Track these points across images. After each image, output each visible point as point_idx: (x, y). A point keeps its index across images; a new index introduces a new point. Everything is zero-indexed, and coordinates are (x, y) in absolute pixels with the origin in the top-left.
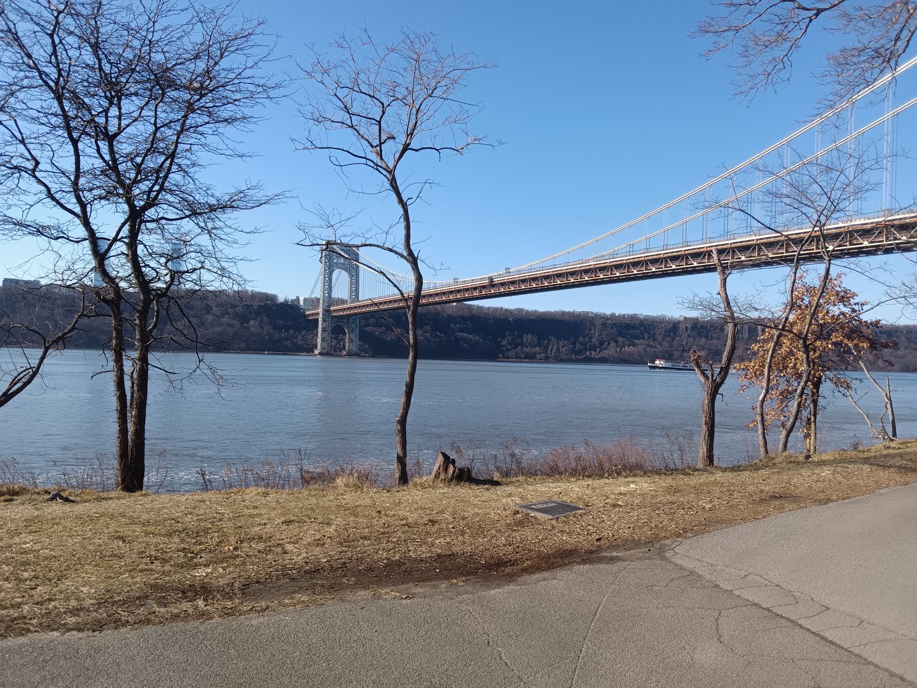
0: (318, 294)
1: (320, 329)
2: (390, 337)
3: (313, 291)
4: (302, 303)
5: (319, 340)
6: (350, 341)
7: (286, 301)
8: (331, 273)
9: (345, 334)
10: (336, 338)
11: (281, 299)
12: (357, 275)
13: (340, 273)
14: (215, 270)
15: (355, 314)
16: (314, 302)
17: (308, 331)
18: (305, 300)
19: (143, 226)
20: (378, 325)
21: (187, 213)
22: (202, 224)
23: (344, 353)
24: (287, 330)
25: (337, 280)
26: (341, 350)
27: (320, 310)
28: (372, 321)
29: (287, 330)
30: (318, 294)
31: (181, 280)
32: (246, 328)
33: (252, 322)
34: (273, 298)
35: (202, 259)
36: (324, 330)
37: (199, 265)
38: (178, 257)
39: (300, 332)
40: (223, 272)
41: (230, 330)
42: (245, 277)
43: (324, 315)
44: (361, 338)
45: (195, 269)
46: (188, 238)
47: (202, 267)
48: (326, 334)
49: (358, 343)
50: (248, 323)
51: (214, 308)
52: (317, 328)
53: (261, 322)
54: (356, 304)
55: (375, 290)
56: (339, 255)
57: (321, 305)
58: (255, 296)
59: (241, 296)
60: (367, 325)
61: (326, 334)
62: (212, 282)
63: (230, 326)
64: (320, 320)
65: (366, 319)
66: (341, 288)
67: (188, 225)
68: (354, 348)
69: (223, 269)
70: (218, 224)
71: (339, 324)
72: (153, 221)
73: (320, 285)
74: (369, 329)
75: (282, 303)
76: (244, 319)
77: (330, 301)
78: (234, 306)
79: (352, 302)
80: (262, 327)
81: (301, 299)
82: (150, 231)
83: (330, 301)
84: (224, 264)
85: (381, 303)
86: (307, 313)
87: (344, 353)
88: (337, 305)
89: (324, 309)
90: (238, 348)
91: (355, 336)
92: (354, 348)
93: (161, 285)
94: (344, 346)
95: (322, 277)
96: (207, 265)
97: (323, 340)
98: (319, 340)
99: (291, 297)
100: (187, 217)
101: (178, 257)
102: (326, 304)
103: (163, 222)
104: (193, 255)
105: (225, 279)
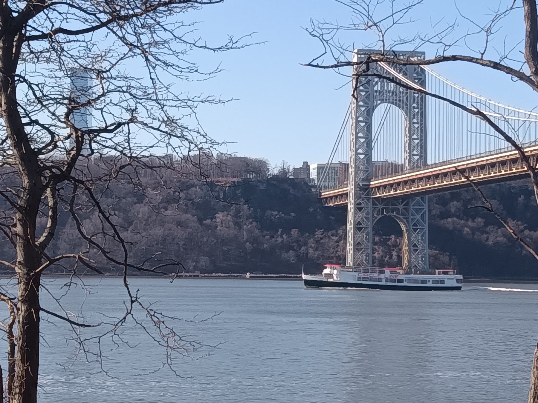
0: (345, 155)
1: (350, 227)
2: (494, 237)
3: (335, 151)
4: (313, 174)
5: (349, 248)
7: (284, 172)
8: (369, 112)
9: (400, 234)
10: (383, 243)
11: (274, 169)
13: (387, 110)
14: (156, 124)
15: (422, 194)
16: (335, 172)
17: (327, 230)
18: (320, 168)
19: (24, 49)
20: (468, 213)
21: (104, 17)
22: (132, 39)
24: (287, 231)
25: (381, 125)
27: (350, 188)
28: (454, 206)
29: (287, 231)
30: (345, 155)
31: (94, 145)
32: (208, 227)
33: (220, 216)
34: (258, 167)
35: (132, 104)
36: (358, 228)
37: (127, 116)
38: (89, 103)
39: (313, 233)
40: (171, 127)
41: (180, 233)
42: (211, 135)
44: (432, 243)
45: (119, 125)
46: (106, 65)
47: (132, 120)
48: (362, 236)
49: (427, 251)
50: (213, 218)
51: (150, 191)
52: (344, 222)
53: (237, 215)
55: (458, 144)
56: (386, 77)
57: (352, 177)
58: (226, 164)
59: (203, 168)
60: (445, 215)
61: (362, 236)
62: (146, 142)
63: (179, 224)
64: (351, 207)
65: (443, 202)
66: (391, 142)
67: (104, 40)
69: (170, 121)
70: (160, 35)
71: (387, 216)
72: (43, 36)
73: (349, 137)
74: (449, 222)
75: (275, 177)
76: (205, 211)
78: (185, 187)
79: (413, 169)
80: (239, 225)
81: (313, 167)
82: (37, 55)
83: (369, 168)
84: (173, 113)
85: (473, 169)
86: (325, 194)
88: (383, 176)
89: (357, 186)
90: (196, 268)
91: (421, 239)
93: (58, 155)
94: (400, 258)
95: (352, 122)
96: (142, 115)
97: (357, 247)
98: (349, 248)
99: (294, 163)
100: (103, 25)
101: (89, 103)
102: (362, 175)
103: (61, 37)
104: (115, 97)
105: (175, 141)
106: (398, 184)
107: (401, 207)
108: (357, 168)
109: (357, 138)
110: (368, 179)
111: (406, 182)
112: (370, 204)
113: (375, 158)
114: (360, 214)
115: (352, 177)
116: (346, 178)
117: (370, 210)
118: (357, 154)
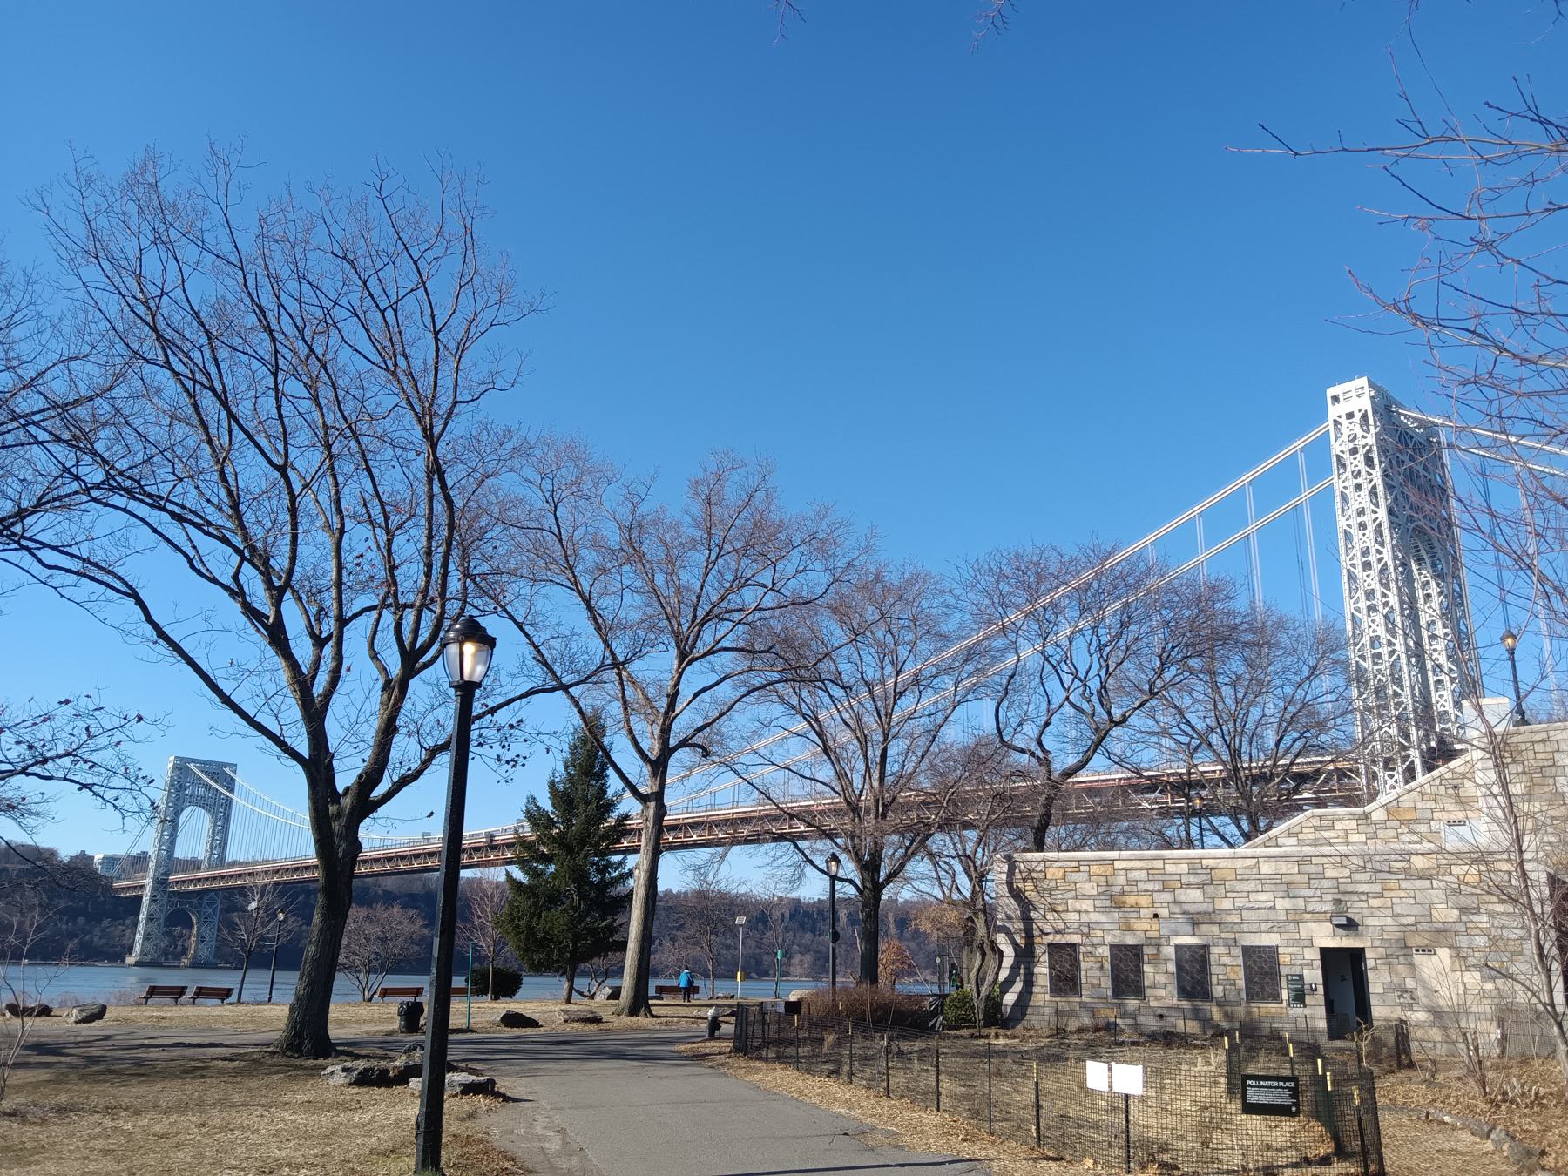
9: (190, 926)
12: (227, 817)
16: (139, 861)
17: (115, 918)
26: (178, 956)
27: (148, 881)
43: (154, 889)
54: (216, 873)
68: (206, 953)
77: (169, 863)
83: (169, 863)
91: (209, 933)
92: (206, 953)
110: (167, 874)
116: (146, 869)
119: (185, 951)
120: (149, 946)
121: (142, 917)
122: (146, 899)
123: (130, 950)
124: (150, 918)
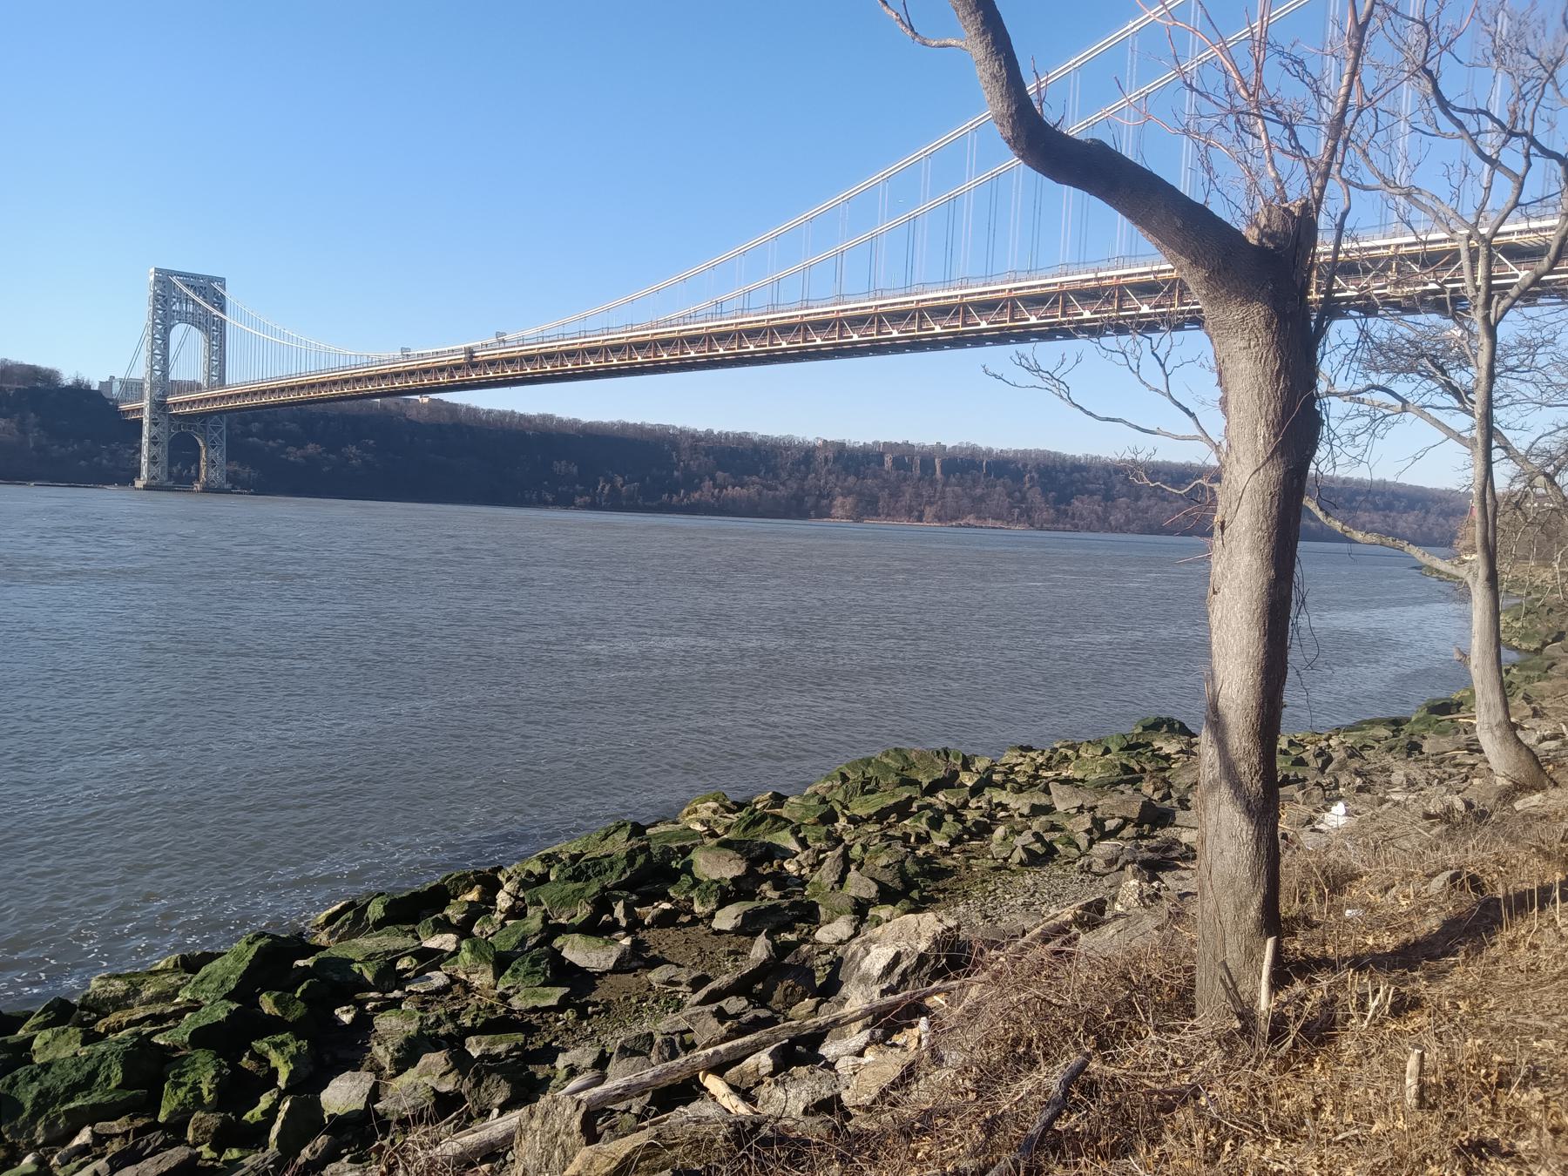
0: (140, 372)
3: (131, 366)
6: (210, 461)
16: (132, 388)
23: (198, 486)
27: (146, 404)
30: (140, 372)
43: (152, 411)
44: (229, 459)
49: (225, 468)
73: (145, 354)
79: (211, 387)
83: (164, 385)
87: (198, 486)
88: (179, 393)
89: (153, 402)
91: (219, 455)
106: (194, 402)
107: (198, 424)
108: (153, 386)
109: (153, 354)
111: (201, 401)
112: (166, 420)
113: (172, 377)
114: (155, 429)
115: (147, 393)
117: (166, 424)
118: (153, 371)
119: (197, 478)
120: (156, 470)
121: (145, 440)
122: (146, 421)
123: (138, 474)
124: (154, 441)
